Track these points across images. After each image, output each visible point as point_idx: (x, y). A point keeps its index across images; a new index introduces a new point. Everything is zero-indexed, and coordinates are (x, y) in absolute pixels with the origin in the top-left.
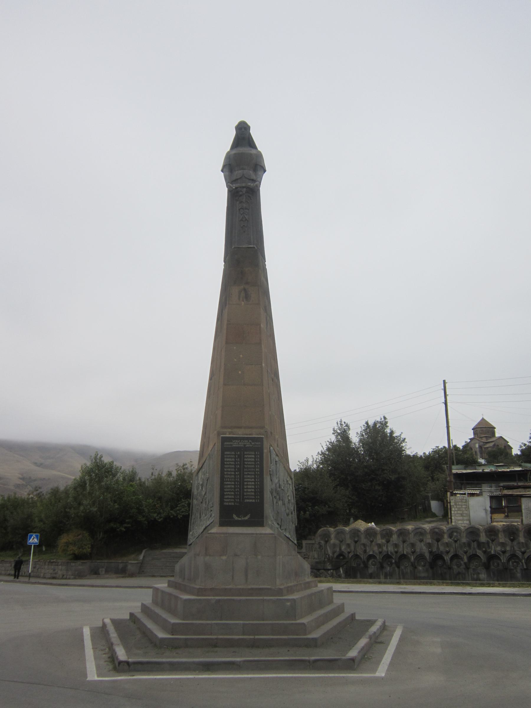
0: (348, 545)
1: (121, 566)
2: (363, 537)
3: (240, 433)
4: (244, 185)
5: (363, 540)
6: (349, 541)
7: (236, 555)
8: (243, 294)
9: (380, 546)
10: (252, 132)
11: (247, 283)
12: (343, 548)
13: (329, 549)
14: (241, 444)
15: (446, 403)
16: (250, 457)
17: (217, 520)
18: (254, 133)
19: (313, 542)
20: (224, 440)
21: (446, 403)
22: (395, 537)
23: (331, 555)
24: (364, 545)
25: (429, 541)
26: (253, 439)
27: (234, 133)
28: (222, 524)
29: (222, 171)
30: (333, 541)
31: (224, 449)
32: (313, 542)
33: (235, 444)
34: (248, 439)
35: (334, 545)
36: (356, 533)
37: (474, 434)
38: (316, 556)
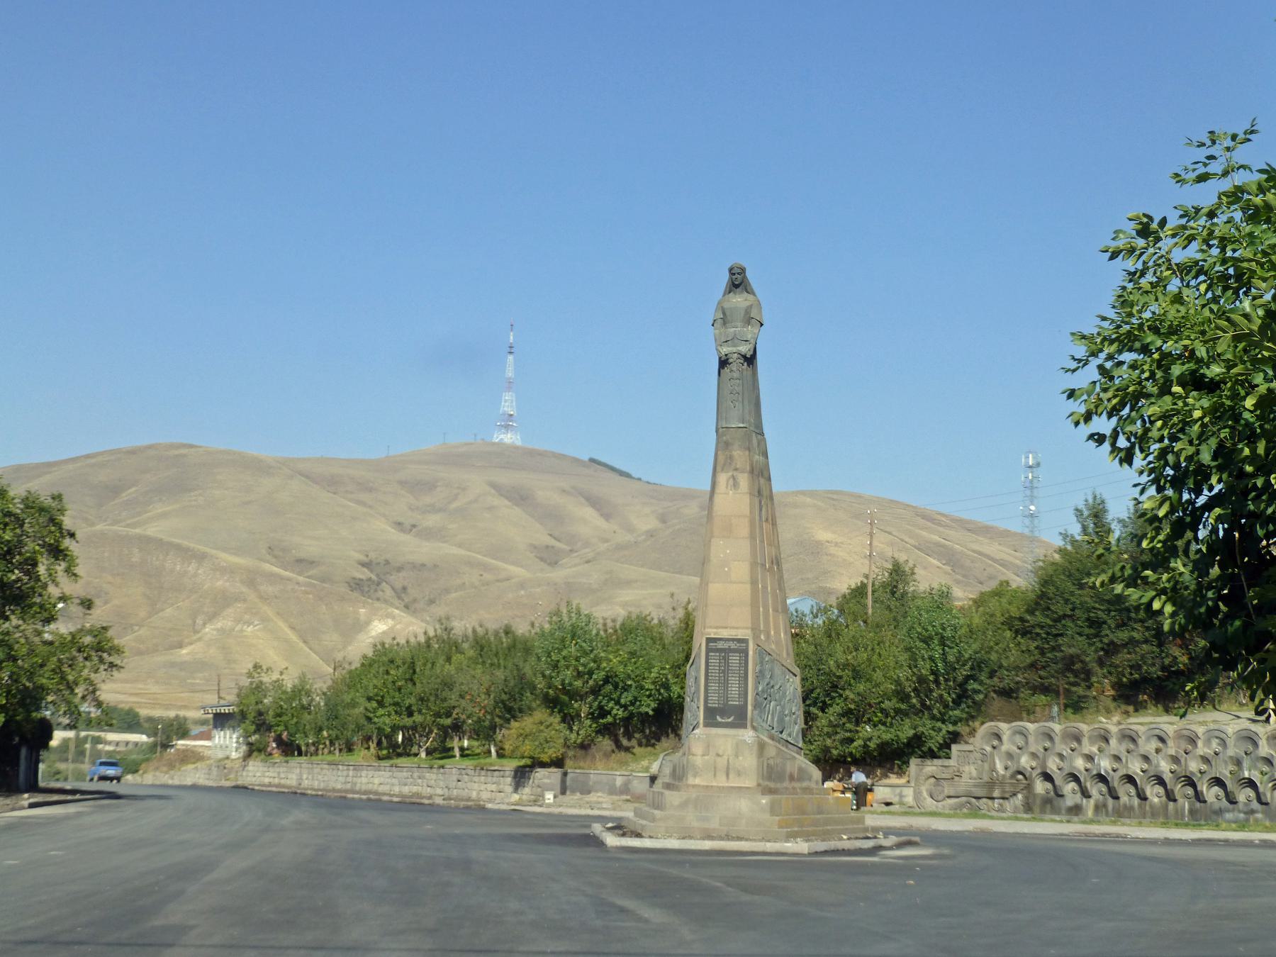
1: (619, 781)
3: (725, 634)
4: (734, 350)
7: (718, 755)
8: (731, 482)
9: (1090, 758)
10: (749, 274)
11: (736, 469)
13: (997, 761)
14: (726, 645)
16: (734, 659)
19: (970, 748)
20: (709, 640)
23: (1002, 772)
25: (1172, 752)
26: (739, 641)
27: (725, 278)
30: (1006, 746)
31: (708, 650)
32: (970, 748)
33: (720, 645)
34: (733, 640)
35: (1010, 756)
38: (974, 773)
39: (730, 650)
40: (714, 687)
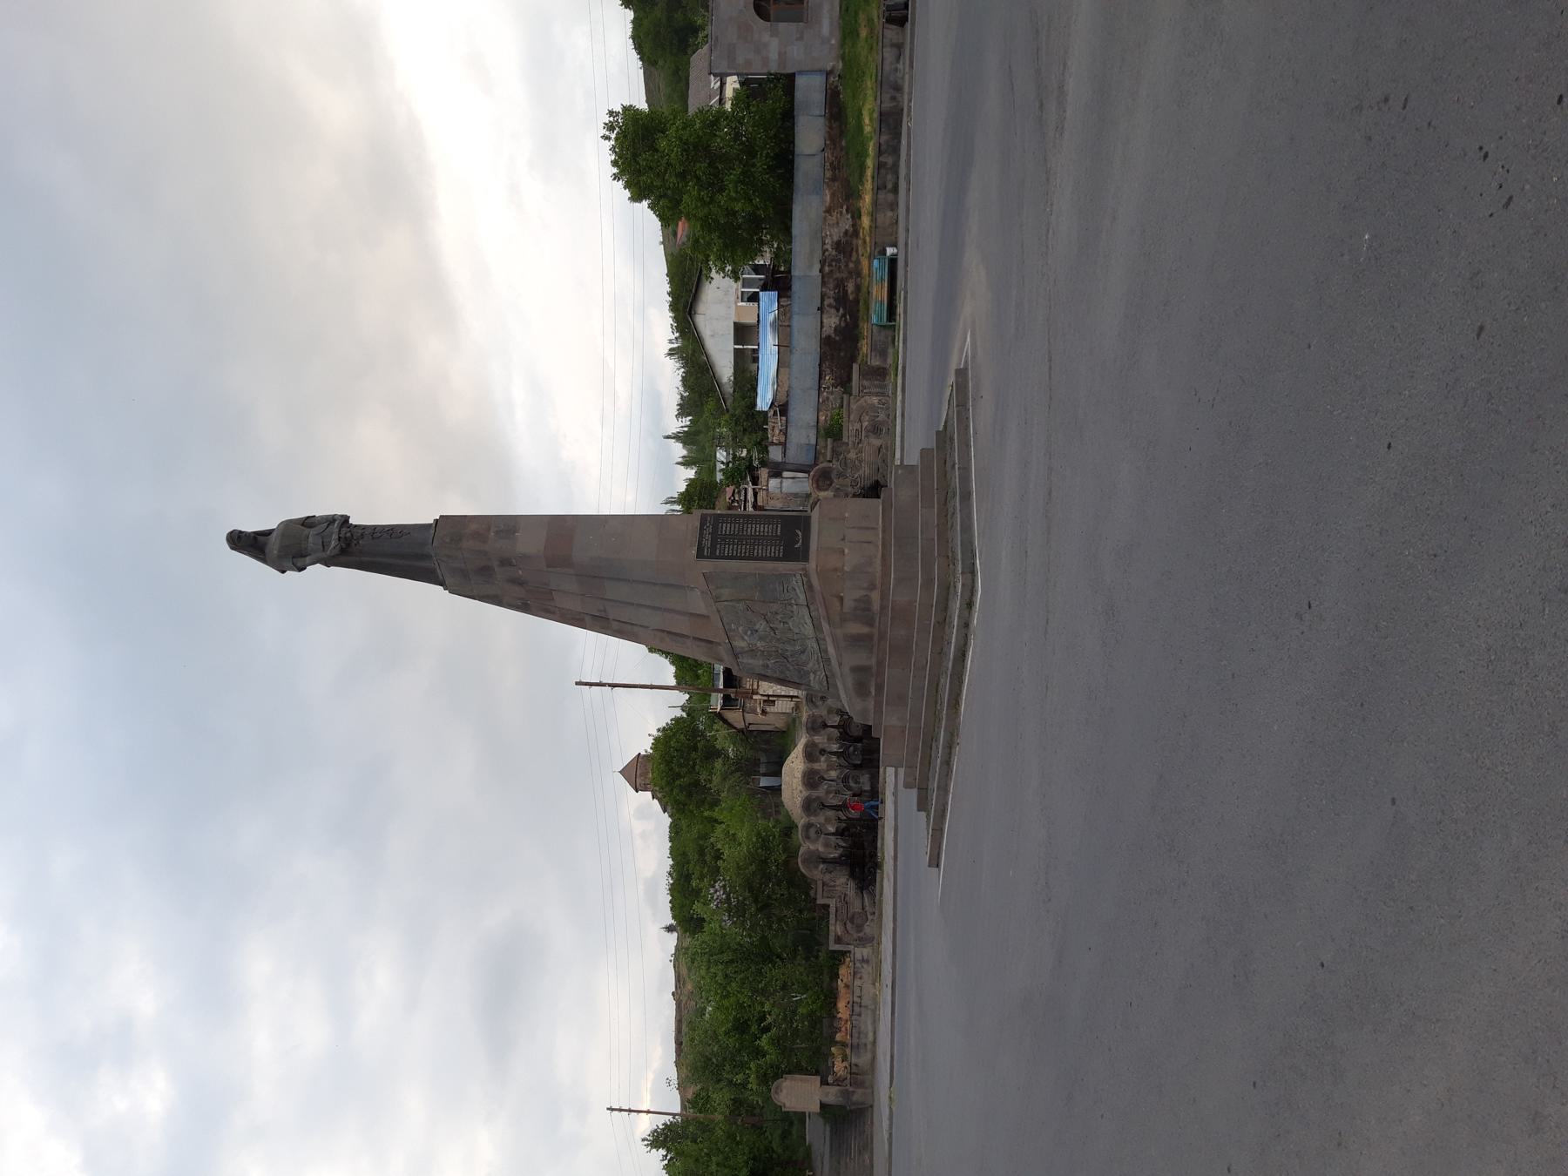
0: (828, 820)
2: (815, 794)
5: (820, 792)
6: (821, 819)
12: (832, 830)
15: (614, 686)
17: (799, 565)
18: (250, 526)
21: (614, 686)
22: (817, 739)
24: (828, 792)
28: (806, 558)
29: (301, 569)
31: (712, 556)
33: (707, 543)
36: (808, 806)
37: (645, 790)
39: (714, 534)
40: (759, 551)
